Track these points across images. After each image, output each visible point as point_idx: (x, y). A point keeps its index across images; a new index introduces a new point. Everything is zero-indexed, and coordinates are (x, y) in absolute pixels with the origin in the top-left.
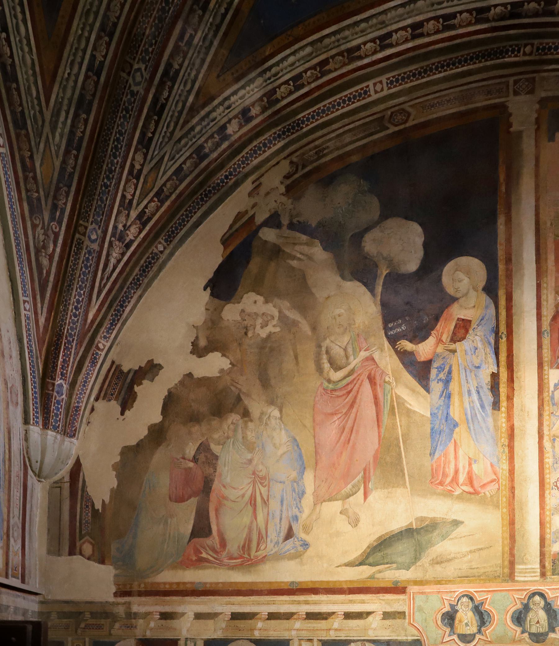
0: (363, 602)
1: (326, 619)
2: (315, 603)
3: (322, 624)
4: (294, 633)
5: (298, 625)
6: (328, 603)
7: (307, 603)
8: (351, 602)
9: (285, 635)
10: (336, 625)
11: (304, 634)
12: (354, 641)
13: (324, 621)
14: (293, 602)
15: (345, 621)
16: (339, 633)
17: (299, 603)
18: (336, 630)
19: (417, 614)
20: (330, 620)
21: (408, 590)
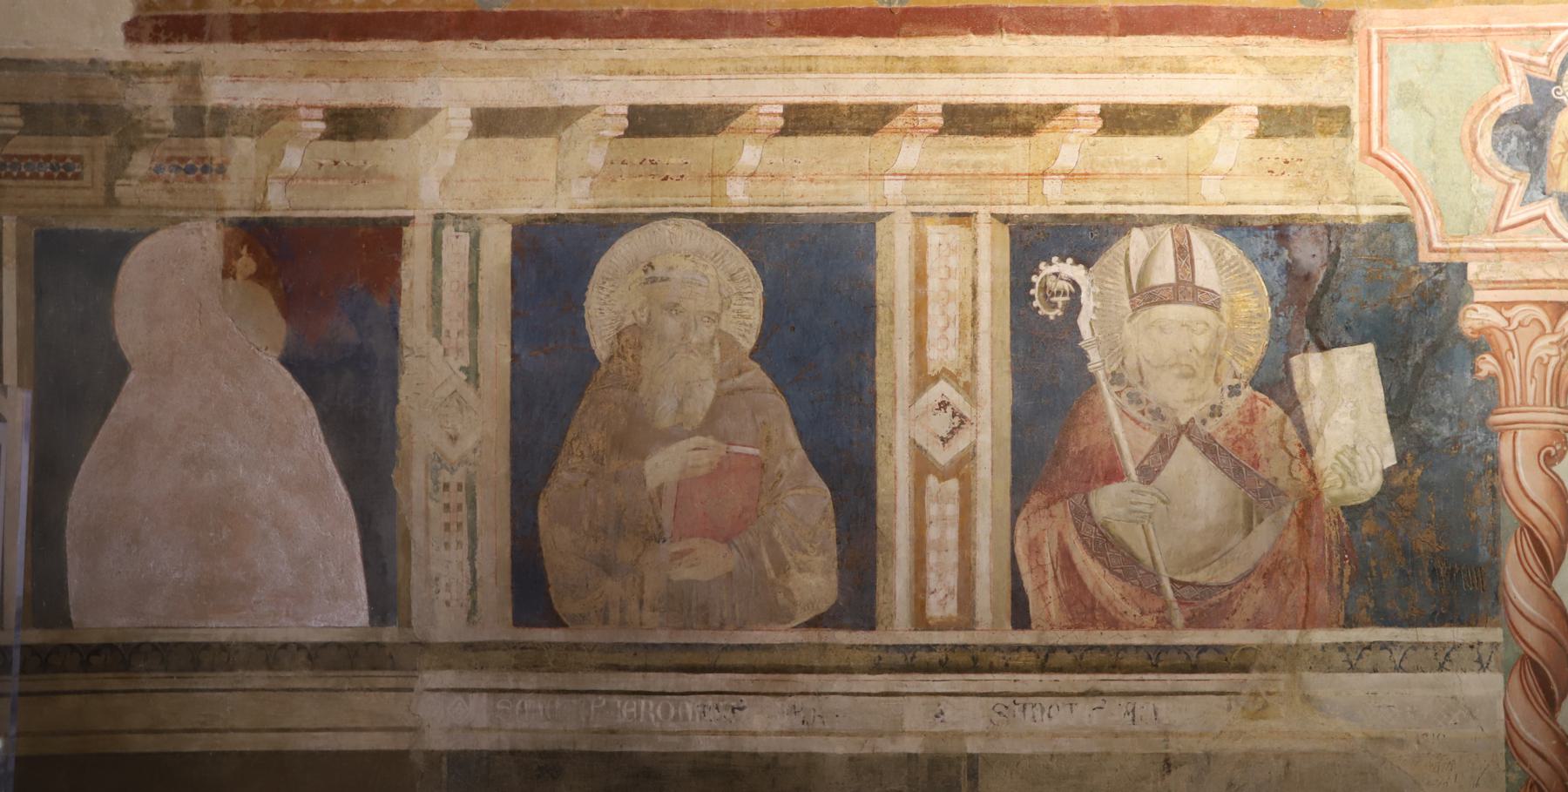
0: (1178, 66)
1: (1028, 131)
2: (983, 68)
3: (1012, 152)
4: (893, 188)
5: (910, 154)
6: (1033, 67)
7: (947, 66)
8: (1129, 64)
9: (857, 198)
10: (1068, 157)
11: (938, 193)
12: (1144, 222)
13: (1018, 142)
14: (890, 64)
15: (1107, 141)
16: (1081, 191)
17: (914, 66)
18: (1069, 176)
19: (1396, 116)
20: (1044, 138)
21: (1358, 24)
